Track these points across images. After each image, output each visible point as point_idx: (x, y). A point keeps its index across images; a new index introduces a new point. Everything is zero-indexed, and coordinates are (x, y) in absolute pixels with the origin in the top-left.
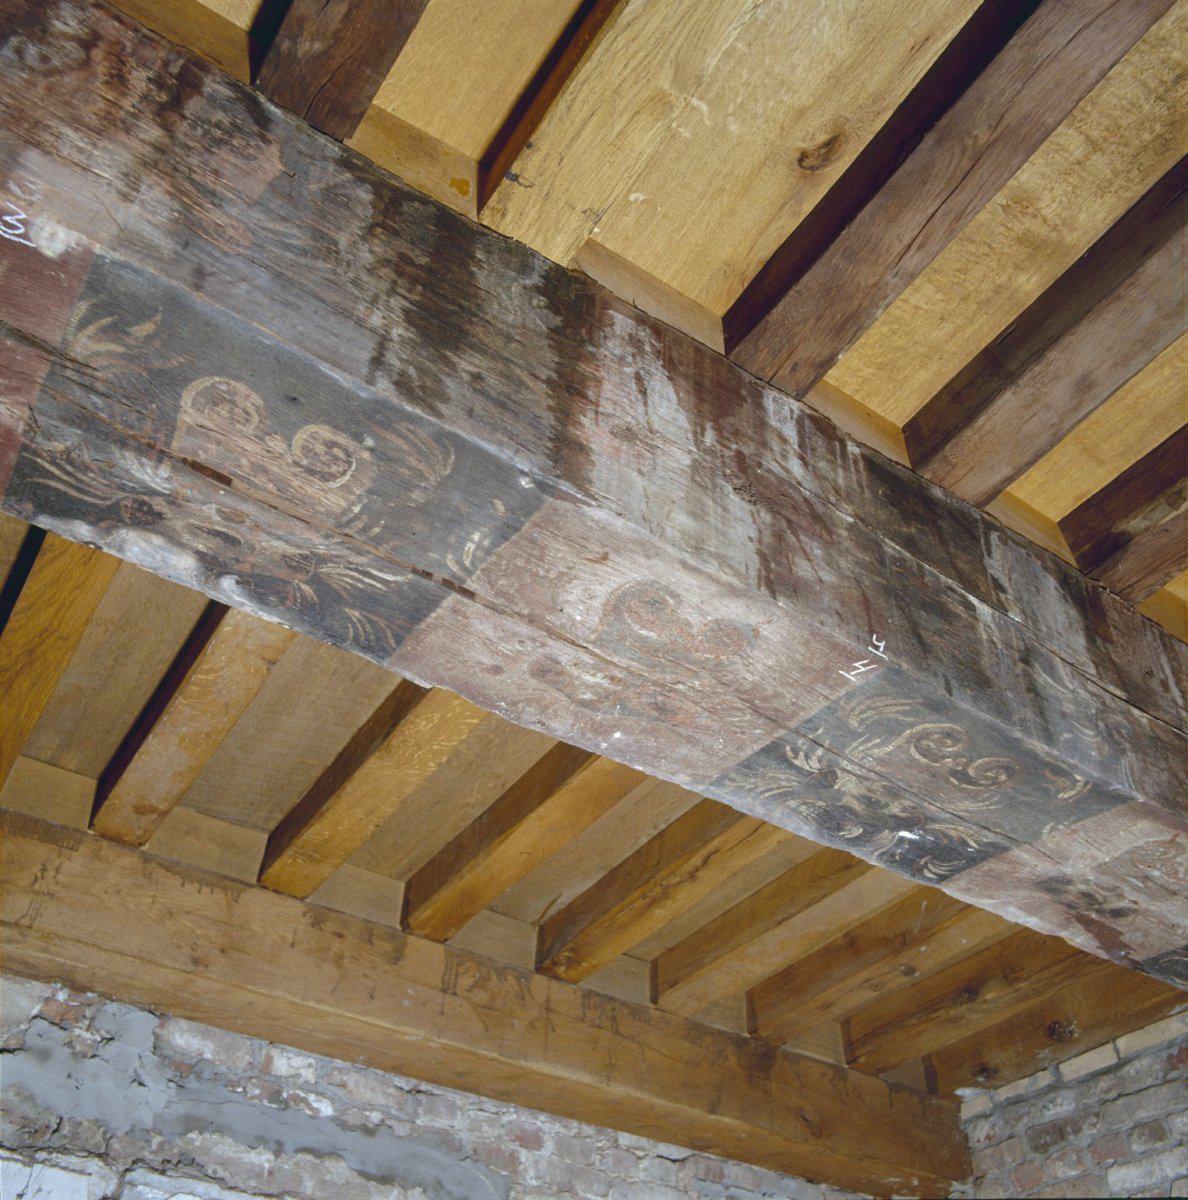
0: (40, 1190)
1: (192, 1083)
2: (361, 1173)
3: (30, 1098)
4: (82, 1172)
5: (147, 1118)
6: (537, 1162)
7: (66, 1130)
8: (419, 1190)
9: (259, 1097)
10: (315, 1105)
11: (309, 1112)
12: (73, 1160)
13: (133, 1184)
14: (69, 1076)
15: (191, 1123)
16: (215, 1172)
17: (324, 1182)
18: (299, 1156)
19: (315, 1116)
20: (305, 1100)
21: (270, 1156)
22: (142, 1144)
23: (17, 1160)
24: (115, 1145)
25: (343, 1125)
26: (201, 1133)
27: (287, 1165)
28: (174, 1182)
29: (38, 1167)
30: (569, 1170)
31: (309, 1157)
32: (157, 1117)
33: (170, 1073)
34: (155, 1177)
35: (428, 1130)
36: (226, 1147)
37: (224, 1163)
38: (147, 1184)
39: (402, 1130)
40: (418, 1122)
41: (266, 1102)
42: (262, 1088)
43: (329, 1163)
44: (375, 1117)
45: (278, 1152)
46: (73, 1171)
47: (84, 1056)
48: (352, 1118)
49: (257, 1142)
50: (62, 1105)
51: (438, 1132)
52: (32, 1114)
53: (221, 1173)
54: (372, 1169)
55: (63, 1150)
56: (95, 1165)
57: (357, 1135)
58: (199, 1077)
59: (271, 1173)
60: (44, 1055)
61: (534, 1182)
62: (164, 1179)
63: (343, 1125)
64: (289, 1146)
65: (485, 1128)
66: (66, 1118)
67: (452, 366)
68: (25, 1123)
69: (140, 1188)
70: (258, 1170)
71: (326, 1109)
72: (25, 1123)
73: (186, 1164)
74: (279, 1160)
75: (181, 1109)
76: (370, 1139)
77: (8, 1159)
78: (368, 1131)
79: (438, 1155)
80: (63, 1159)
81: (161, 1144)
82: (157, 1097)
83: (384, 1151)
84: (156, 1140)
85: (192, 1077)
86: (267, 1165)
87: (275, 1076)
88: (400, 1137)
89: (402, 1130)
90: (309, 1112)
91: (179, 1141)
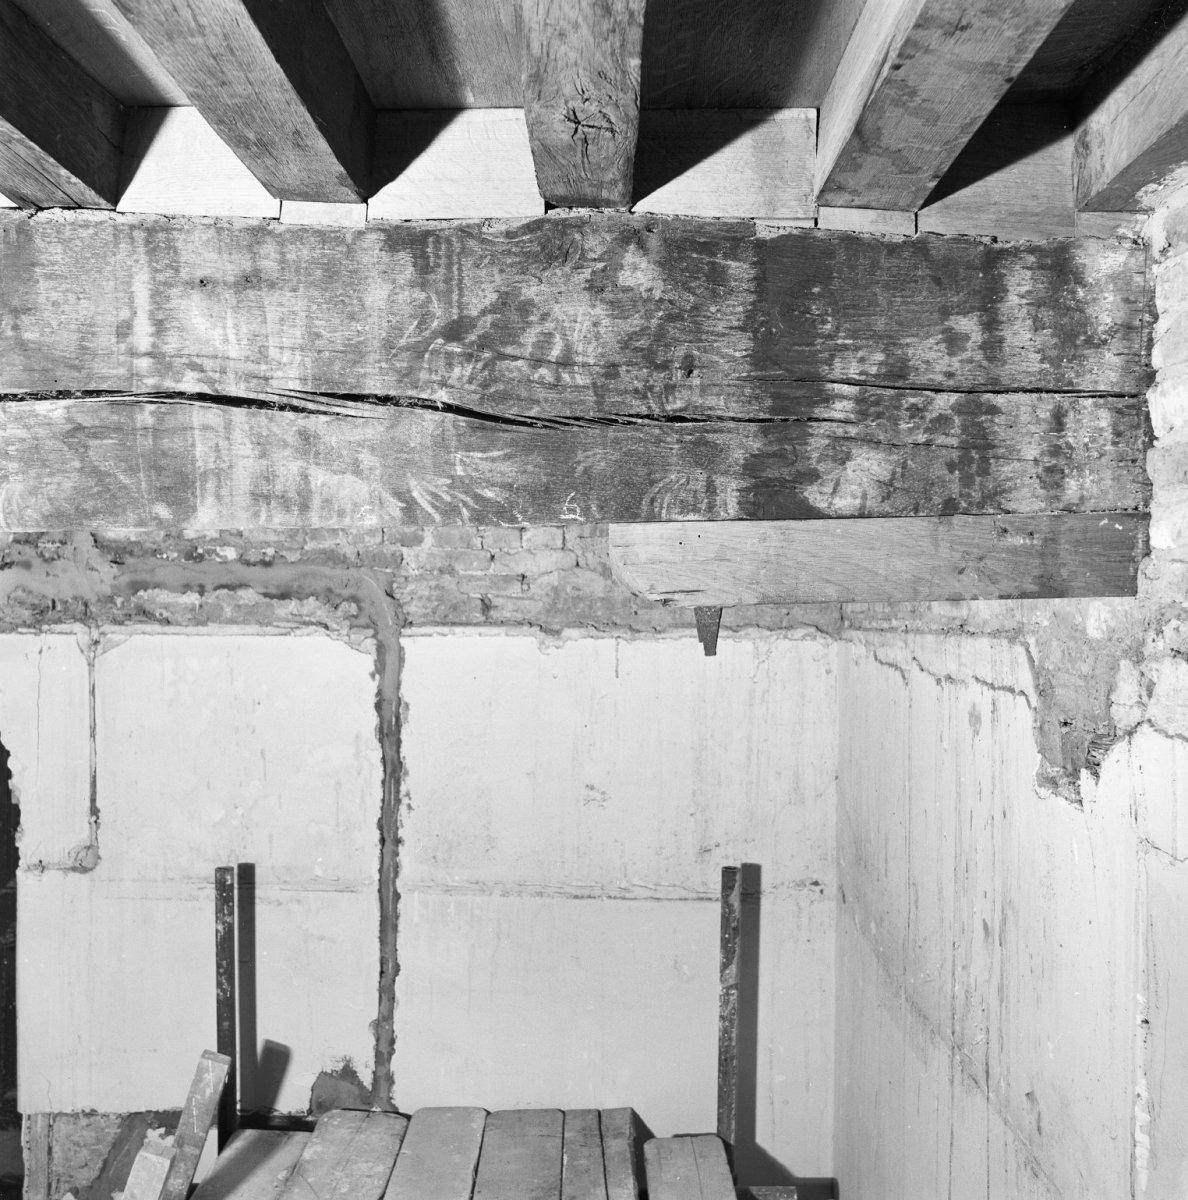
0: (49, 648)
1: (129, 560)
2: (265, 595)
3: (30, 592)
4: (71, 633)
5: (107, 590)
6: (417, 556)
8: (312, 599)
9: (178, 558)
10: (222, 553)
11: (218, 560)
14: (48, 574)
15: (136, 587)
16: (161, 614)
17: (239, 606)
18: (218, 592)
19: (225, 562)
20: (214, 551)
21: (197, 595)
22: (110, 605)
23: (30, 633)
25: (248, 563)
26: (145, 590)
27: (210, 598)
28: (129, 628)
29: (43, 636)
30: (449, 556)
31: (225, 591)
32: (112, 587)
33: (110, 557)
34: (117, 628)
35: (314, 551)
36: (163, 596)
38: (113, 633)
39: (292, 557)
40: (306, 547)
41: (183, 560)
42: (179, 551)
43: (241, 593)
44: (270, 551)
45: (202, 590)
46: (66, 633)
47: (53, 559)
48: (253, 556)
49: (186, 588)
50: (51, 593)
51: (324, 552)
52: (36, 602)
53: (166, 614)
54: (273, 591)
55: (59, 621)
56: (78, 627)
57: (259, 569)
58: (131, 553)
59: (201, 606)
60: (27, 565)
61: (416, 572)
62: (123, 628)
63: (248, 563)
64: (209, 587)
65: (367, 538)
66: (56, 600)
68: (34, 607)
69: (109, 636)
70: (190, 607)
71: (230, 553)
73: (145, 614)
74: (204, 598)
75: (125, 579)
76: (269, 569)
77: (26, 633)
78: (267, 564)
79: (326, 570)
81: (123, 603)
82: (106, 576)
83: (280, 575)
84: (119, 601)
85: (127, 556)
86: (197, 603)
87: (188, 540)
88: (292, 563)
89: (292, 557)
90: (218, 560)
91: (133, 599)
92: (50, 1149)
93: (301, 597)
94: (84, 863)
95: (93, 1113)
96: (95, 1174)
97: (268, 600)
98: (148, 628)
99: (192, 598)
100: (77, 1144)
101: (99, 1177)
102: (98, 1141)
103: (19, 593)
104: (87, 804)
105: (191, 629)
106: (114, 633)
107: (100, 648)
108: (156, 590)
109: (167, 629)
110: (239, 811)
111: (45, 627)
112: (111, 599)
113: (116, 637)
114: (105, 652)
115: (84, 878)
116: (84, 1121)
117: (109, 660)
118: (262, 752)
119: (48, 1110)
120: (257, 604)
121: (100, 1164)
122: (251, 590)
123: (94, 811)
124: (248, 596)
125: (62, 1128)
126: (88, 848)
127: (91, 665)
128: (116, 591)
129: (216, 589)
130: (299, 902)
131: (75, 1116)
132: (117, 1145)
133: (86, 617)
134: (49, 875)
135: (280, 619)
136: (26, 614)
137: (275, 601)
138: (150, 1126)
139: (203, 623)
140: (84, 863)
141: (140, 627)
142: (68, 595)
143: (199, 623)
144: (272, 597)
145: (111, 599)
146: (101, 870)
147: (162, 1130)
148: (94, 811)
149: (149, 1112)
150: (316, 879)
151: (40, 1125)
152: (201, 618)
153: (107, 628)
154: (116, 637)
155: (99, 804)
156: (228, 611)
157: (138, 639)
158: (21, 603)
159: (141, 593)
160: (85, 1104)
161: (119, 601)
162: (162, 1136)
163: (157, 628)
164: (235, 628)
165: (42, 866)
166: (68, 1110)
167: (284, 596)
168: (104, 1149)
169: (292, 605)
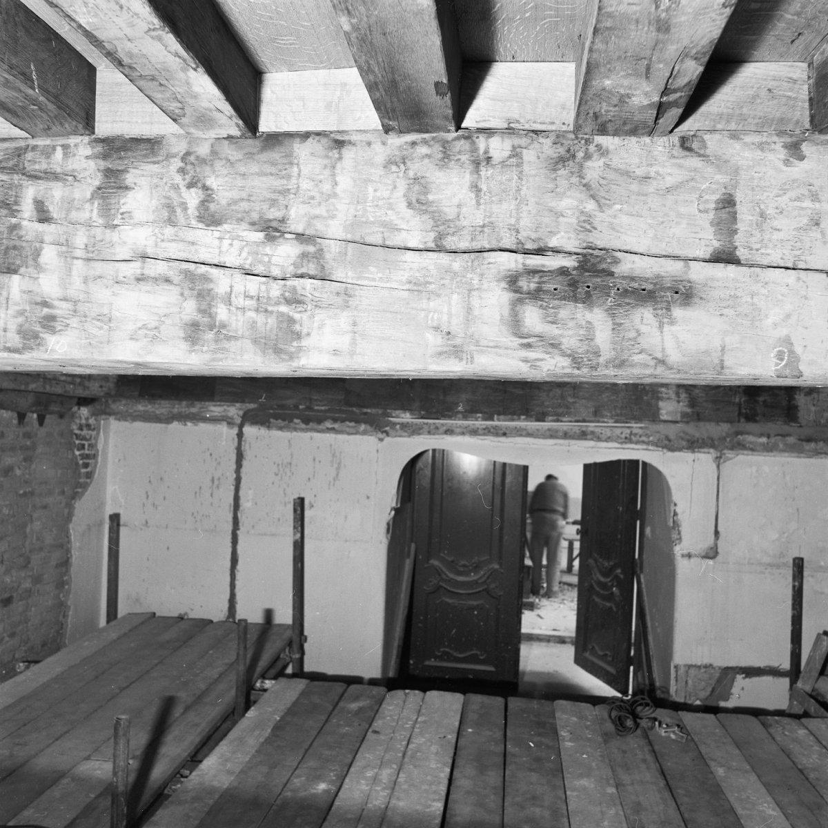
2: (799, 440)
3: (687, 434)
5: (724, 434)
7: (700, 441)
8: (821, 443)
12: (706, 450)
13: (724, 454)
15: (737, 433)
24: (716, 443)
27: (773, 440)
31: (780, 437)
34: (730, 452)
36: (751, 438)
37: (751, 443)
43: (788, 438)
45: (769, 437)
49: (761, 435)
50: (697, 435)
53: (751, 446)
54: (802, 437)
55: (701, 447)
64: (772, 435)
67: (757, 402)
72: (688, 441)
80: (703, 450)
84: (728, 440)
92: (686, 682)
93: (816, 441)
94: (712, 554)
95: (711, 665)
96: (708, 693)
97: (800, 442)
98: (746, 452)
99: (764, 440)
100: (700, 679)
101: (710, 695)
102: (710, 679)
103: (682, 434)
104: (713, 528)
105: (765, 454)
106: (729, 454)
107: (722, 461)
108: (747, 436)
109: (754, 453)
110: (786, 535)
111: (696, 450)
112: (725, 439)
113: (730, 456)
114: (725, 462)
115: (711, 562)
116: (703, 670)
117: (727, 467)
118: (798, 510)
119: (690, 663)
120: (795, 444)
121: (711, 689)
122: (792, 438)
123: (717, 533)
124: (791, 440)
125: (692, 672)
126: (712, 548)
127: (718, 467)
128: (728, 435)
129: (778, 435)
130: (812, 576)
131: (699, 667)
132: (719, 681)
133: (713, 446)
134: (692, 560)
135: (809, 451)
136: (684, 443)
137: (804, 443)
138: (738, 673)
139: (771, 451)
140: (712, 554)
141: (741, 452)
142: (705, 436)
143: (768, 451)
144: (802, 440)
145: (725, 439)
146: (719, 558)
147: (744, 675)
148: (717, 533)
149: (737, 667)
150: (821, 567)
151: (682, 671)
152: (768, 449)
153: (725, 451)
154: (730, 456)
155: (719, 529)
156: (781, 446)
157: (741, 457)
158: (682, 439)
159: (739, 437)
160: (706, 661)
161: (728, 440)
162: (744, 678)
163: (750, 452)
164: (786, 454)
165: (689, 556)
166: (699, 664)
167: (809, 440)
168: (713, 682)
169: (813, 445)
